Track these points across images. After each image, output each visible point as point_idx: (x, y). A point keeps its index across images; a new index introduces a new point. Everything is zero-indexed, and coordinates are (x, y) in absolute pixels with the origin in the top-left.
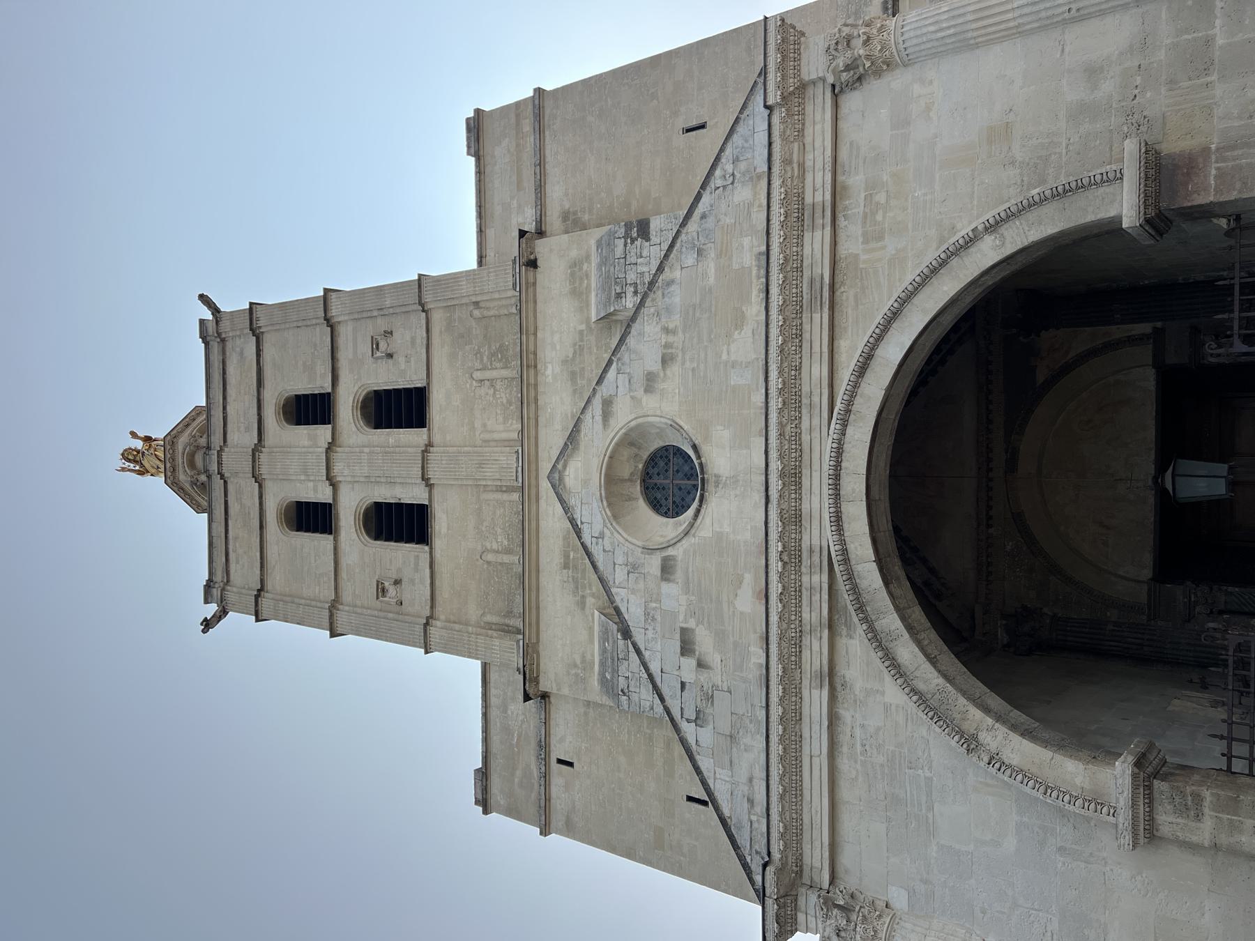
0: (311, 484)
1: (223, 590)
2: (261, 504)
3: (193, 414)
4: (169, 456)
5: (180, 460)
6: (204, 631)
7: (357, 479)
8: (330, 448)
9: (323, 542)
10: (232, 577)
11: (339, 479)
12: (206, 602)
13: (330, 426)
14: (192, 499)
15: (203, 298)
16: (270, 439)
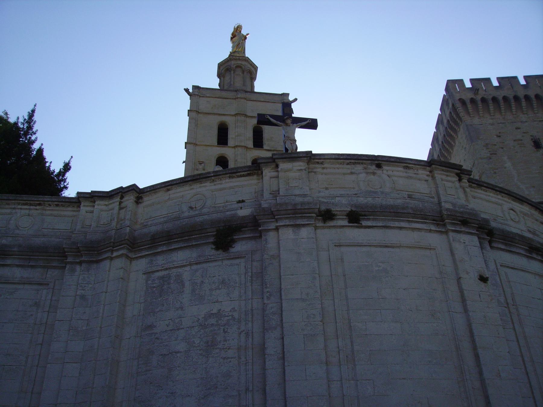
0: (234, 137)
1: (198, 95)
2: (227, 115)
3: (255, 67)
4: (241, 58)
5: (239, 62)
6: (185, 89)
7: (236, 156)
8: (246, 147)
9: (215, 140)
10: (201, 98)
11: (236, 149)
12: (193, 86)
13: (252, 147)
14: (224, 64)
15: (296, 100)
16: (248, 120)
